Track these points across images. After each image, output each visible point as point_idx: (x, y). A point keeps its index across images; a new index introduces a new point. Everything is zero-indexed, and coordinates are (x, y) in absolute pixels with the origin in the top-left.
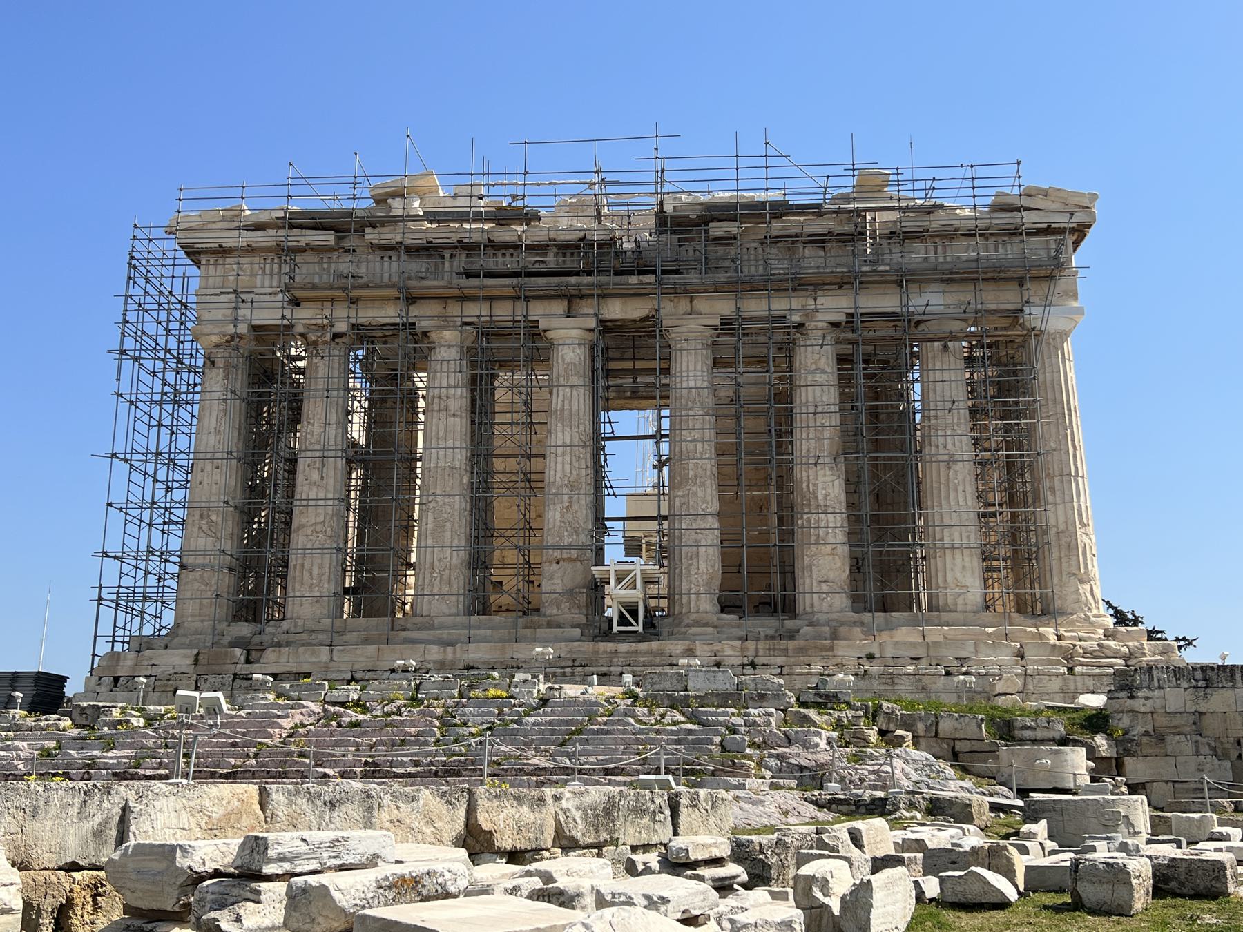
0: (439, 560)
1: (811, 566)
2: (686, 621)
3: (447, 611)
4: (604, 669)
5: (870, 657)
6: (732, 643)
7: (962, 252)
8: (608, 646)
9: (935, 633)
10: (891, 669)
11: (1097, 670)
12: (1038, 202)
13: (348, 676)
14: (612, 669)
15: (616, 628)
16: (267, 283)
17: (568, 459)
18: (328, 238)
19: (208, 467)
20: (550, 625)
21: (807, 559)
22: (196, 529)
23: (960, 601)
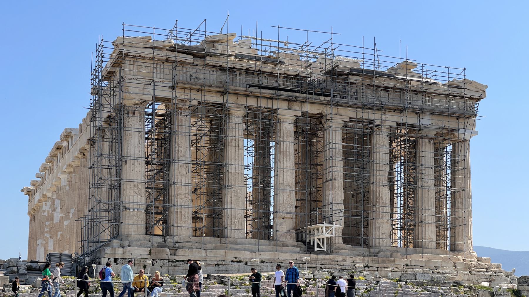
0: (238, 214)
1: (379, 227)
2: (335, 247)
3: (241, 236)
4: (314, 265)
5: (407, 265)
6: (359, 257)
7: (441, 103)
8: (314, 256)
9: (426, 257)
10: (415, 270)
11: (479, 273)
12: (467, 86)
13: (216, 263)
14: (317, 265)
15: (316, 249)
16: (159, 76)
17: (289, 173)
18: (189, 58)
19: (136, 163)
20: (284, 245)
21: (377, 224)
22: (132, 192)
23: (430, 244)
